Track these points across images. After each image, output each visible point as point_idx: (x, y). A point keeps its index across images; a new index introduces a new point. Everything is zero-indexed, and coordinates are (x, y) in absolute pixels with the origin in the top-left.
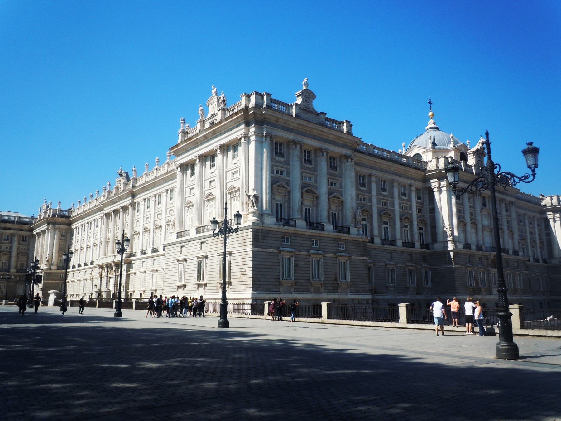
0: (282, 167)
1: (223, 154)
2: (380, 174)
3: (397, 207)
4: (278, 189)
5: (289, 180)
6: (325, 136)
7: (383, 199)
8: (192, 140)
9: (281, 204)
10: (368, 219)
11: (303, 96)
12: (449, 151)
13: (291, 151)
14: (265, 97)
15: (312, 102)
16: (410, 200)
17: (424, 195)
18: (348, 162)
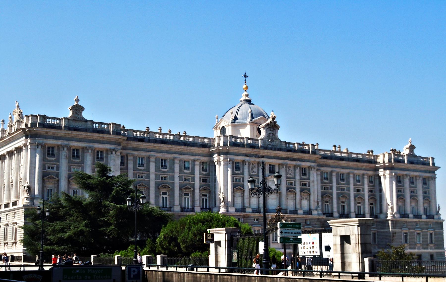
0: (53, 164)
1: (18, 153)
2: (160, 155)
3: (177, 181)
4: (49, 180)
5: (59, 173)
6: (90, 138)
7: (162, 174)
8: (4, 140)
9: (51, 190)
10: (145, 191)
11: (74, 110)
12: (247, 125)
13: (61, 152)
14: (38, 117)
15: (81, 113)
16: (193, 172)
17: (211, 167)
18: (112, 154)
